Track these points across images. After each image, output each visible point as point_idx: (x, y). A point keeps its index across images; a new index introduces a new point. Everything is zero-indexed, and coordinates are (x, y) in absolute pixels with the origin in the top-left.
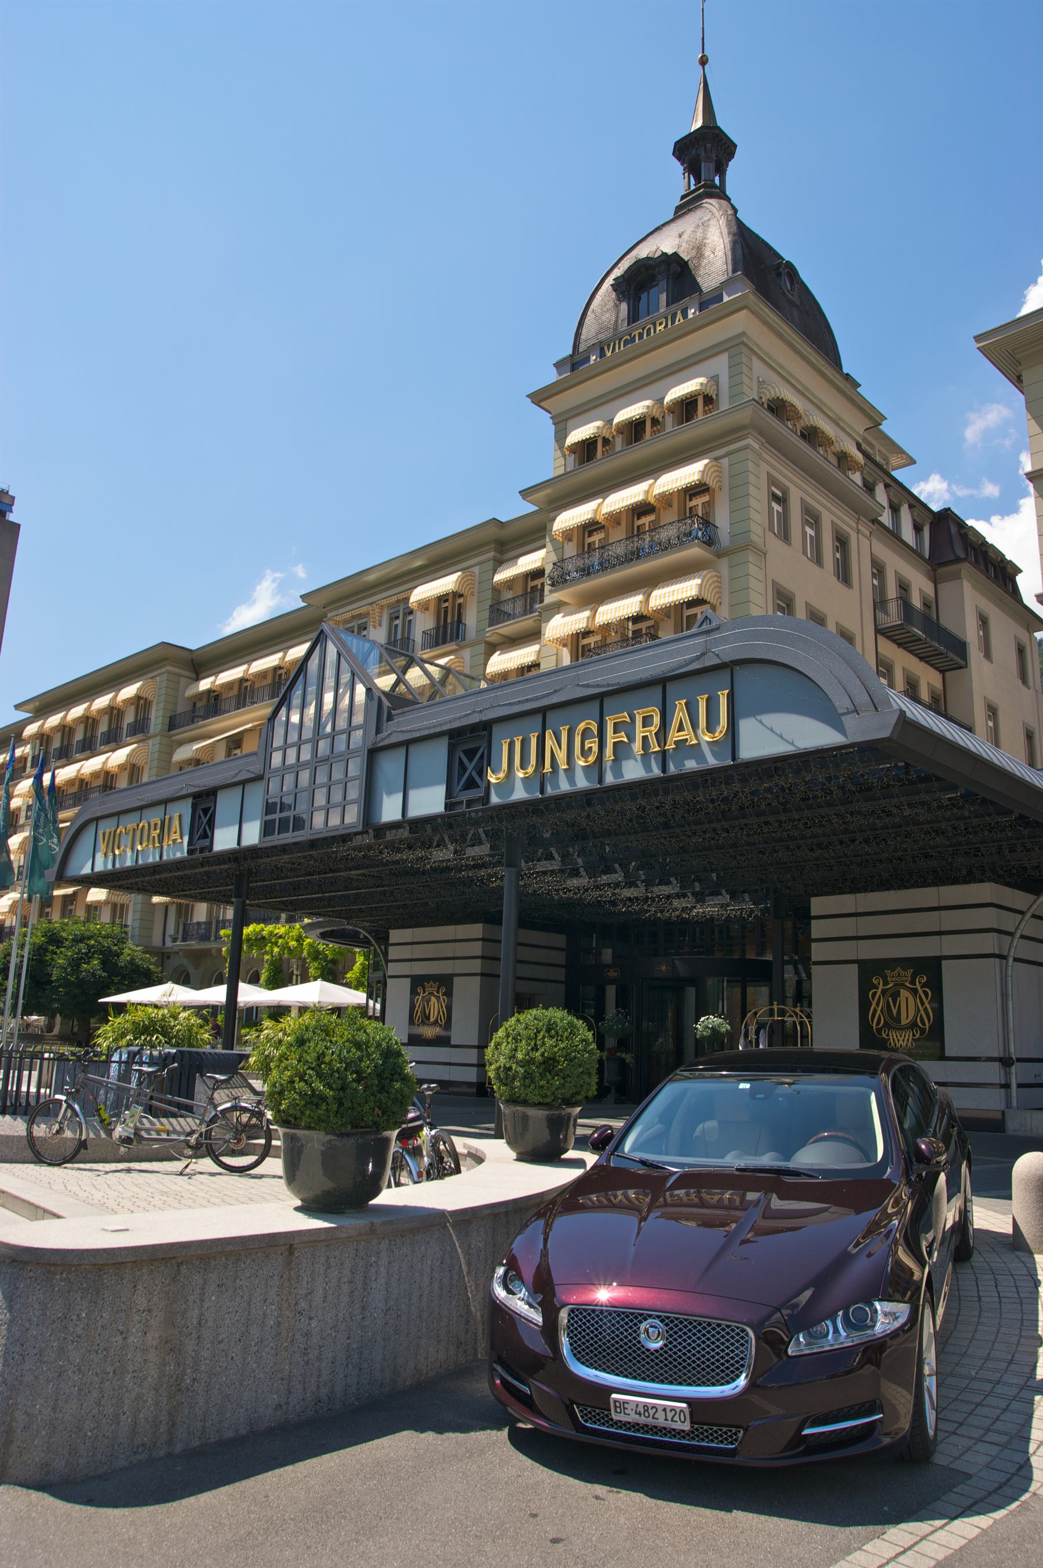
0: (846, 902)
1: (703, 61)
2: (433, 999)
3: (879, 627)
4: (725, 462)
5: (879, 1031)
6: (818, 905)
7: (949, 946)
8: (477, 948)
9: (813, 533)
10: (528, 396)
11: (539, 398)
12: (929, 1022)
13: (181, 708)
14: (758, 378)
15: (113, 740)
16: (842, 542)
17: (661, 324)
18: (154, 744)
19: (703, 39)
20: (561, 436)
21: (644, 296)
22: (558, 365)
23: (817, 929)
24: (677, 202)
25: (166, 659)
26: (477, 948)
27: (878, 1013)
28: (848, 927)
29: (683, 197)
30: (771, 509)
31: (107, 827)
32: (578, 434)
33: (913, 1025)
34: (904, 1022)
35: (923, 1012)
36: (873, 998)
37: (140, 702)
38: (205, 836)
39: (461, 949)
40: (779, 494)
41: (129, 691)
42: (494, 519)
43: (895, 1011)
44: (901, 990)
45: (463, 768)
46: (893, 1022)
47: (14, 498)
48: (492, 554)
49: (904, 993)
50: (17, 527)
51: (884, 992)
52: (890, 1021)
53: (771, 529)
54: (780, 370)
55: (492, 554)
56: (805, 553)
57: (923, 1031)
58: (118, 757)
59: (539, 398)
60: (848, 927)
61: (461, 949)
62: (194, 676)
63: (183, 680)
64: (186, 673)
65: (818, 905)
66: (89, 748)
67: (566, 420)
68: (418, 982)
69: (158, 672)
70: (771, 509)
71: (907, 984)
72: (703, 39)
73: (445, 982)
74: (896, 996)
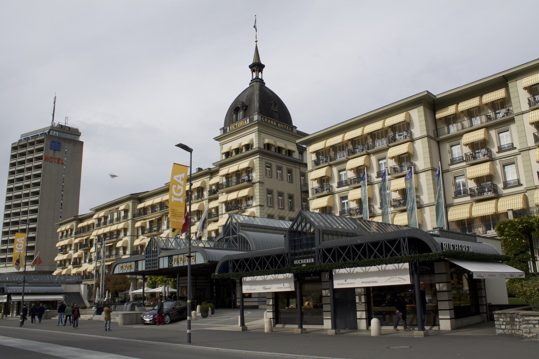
1: (256, 41)
9: (280, 172)
13: (137, 212)
16: (290, 171)
18: (130, 222)
21: (239, 114)
22: (221, 129)
29: (251, 81)
30: (266, 170)
31: (121, 265)
38: (137, 268)
40: (269, 165)
47: (81, 133)
50: (82, 143)
53: (266, 175)
55: (209, 176)
62: (139, 202)
63: (136, 203)
64: (137, 201)
70: (266, 170)
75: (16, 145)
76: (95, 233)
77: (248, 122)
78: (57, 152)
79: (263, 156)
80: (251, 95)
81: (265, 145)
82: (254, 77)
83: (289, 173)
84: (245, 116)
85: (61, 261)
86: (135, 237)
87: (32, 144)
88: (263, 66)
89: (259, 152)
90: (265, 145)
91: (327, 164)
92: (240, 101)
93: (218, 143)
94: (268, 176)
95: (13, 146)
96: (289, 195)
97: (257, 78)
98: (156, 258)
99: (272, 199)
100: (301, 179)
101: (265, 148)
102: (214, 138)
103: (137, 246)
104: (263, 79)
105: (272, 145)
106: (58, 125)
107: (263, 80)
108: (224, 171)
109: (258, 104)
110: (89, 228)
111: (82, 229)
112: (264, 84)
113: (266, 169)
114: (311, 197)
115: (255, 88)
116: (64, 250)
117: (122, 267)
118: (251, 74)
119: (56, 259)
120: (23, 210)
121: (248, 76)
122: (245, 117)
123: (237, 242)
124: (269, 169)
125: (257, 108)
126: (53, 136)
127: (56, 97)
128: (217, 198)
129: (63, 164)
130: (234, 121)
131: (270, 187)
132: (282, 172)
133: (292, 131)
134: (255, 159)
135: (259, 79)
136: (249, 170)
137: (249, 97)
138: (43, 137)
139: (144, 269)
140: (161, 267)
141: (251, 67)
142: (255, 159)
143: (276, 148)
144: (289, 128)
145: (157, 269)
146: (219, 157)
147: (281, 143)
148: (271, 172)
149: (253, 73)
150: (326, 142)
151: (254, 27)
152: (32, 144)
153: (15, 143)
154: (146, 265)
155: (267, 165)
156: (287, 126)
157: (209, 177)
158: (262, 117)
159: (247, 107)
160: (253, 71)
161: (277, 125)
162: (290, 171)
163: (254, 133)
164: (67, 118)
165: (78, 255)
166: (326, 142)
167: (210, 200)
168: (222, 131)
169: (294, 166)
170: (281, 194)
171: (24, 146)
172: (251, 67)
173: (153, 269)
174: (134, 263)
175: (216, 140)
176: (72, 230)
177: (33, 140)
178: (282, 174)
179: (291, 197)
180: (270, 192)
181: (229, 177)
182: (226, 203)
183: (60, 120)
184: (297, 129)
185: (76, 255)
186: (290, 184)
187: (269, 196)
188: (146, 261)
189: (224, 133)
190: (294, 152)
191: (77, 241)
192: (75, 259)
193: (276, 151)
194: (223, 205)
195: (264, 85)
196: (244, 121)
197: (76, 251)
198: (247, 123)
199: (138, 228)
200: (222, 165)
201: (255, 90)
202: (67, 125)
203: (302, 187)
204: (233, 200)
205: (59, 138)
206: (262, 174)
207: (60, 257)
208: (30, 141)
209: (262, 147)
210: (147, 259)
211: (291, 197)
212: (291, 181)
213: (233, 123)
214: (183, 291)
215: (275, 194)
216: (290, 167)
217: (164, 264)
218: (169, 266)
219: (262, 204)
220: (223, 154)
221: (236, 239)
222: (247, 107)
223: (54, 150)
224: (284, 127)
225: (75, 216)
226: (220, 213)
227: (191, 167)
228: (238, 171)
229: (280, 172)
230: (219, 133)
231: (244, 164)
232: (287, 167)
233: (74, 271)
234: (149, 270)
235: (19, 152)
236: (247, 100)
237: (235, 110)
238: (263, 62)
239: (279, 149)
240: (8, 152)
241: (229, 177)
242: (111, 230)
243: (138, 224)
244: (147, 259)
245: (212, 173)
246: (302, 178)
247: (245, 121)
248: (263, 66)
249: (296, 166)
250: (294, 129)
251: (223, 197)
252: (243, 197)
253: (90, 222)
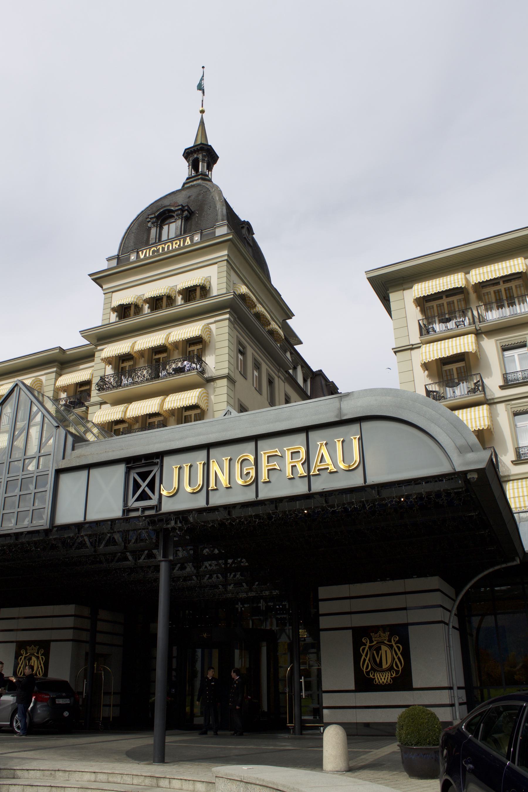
0: (344, 590)
1: (202, 112)
2: (34, 658)
5: (368, 673)
6: (323, 592)
7: (412, 616)
10: (89, 275)
12: (401, 666)
16: (271, 382)
17: (176, 243)
19: (202, 101)
23: (323, 607)
27: (367, 661)
28: (345, 606)
29: (188, 179)
33: (391, 669)
34: (385, 666)
35: (397, 660)
36: (363, 652)
43: (378, 660)
44: (382, 646)
45: (137, 486)
46: (377, 666)
49: (384, 648)
51: (370, 647)
52: (375, 667)
55: (55, 369)
56: (253, 385)
57: (397, 672)
60: (345, 606)
65: (323, 592)
71: (386, 642)
72: (202, 101)
74: (378, 649)
102: (90, 275)
122: (185, 232)
134: (216, 322)
141: (188, 154)
142: (216, 322)
151: (200, 87)
159: (191, 213)
163: (216, 266)
189: (118, 264)
218: (127, 510)
220: (114, 310)
222: (191, 213)
237: (158, 217)
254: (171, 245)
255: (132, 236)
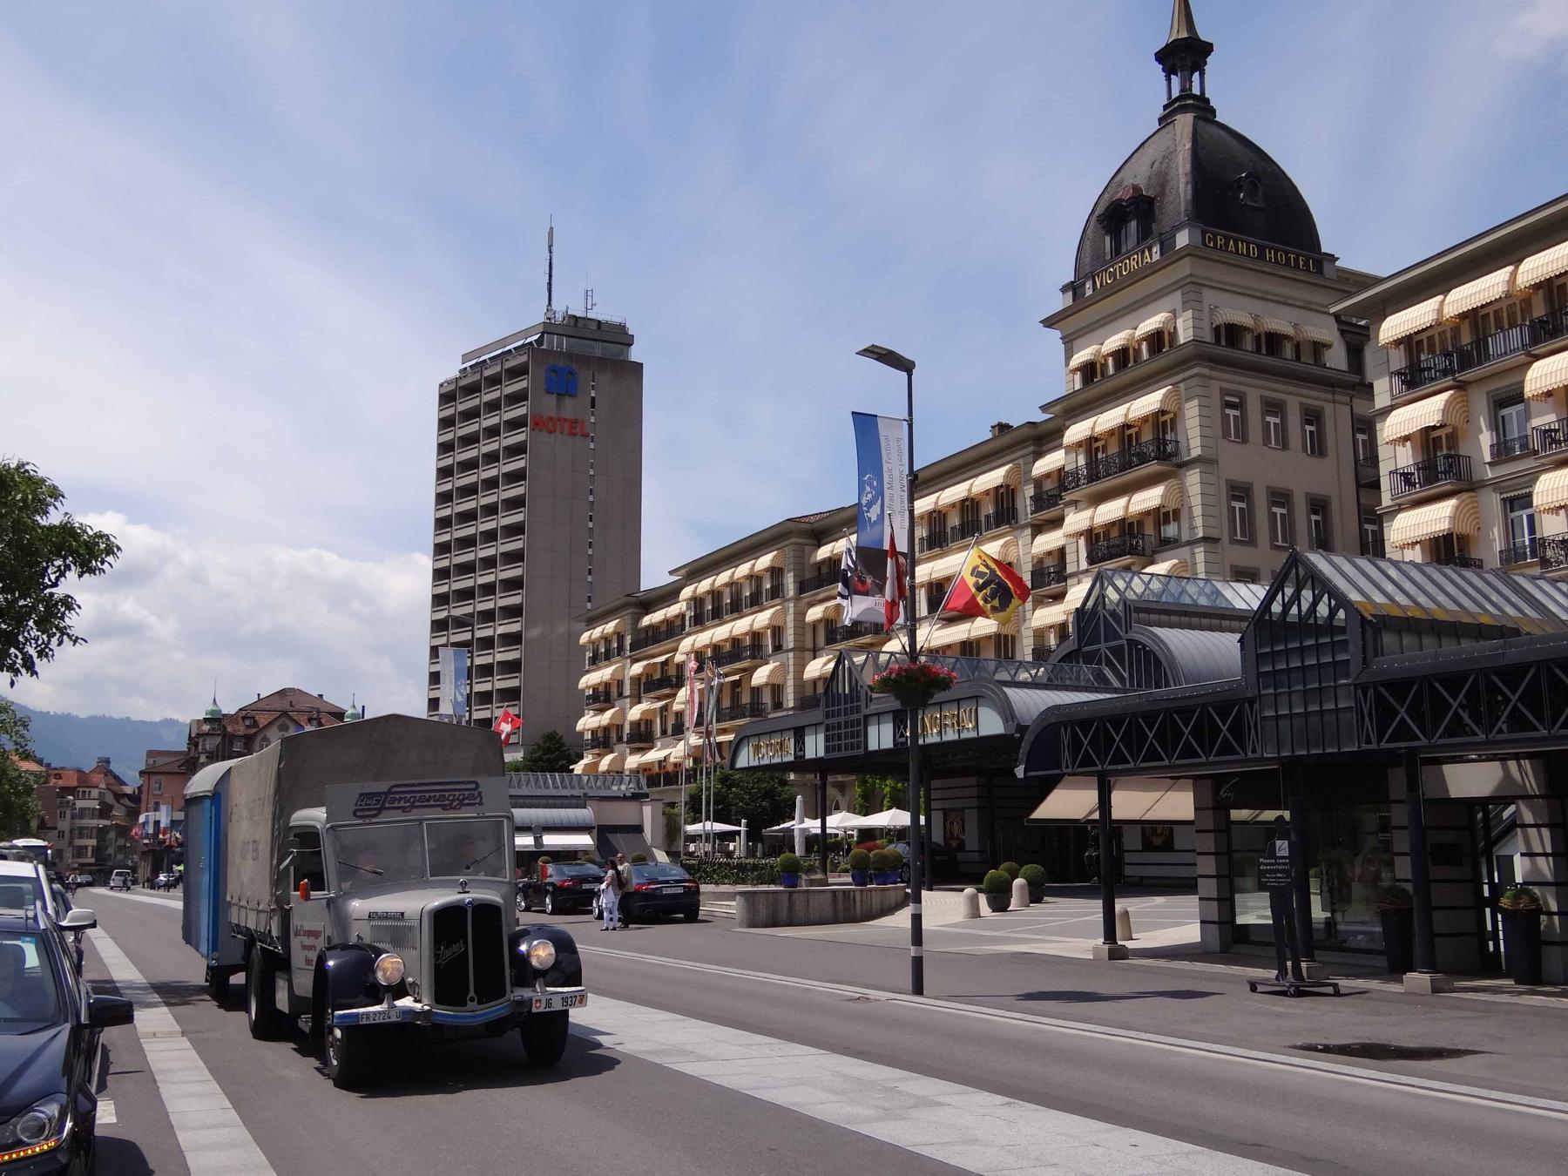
3: (1362, 482)
4: (1182, 386)
8: (974, 792)
11: (1049, 322)
14: (1210, 306)
15: (756, 602)
16: (1312, 416)
20: (1069, 357)
21: (1123, 231)
22: (1064, 290)
24: (1160, 112)
25: (791, 532)
26: (974, 792)
29: (1165, 107)
30: (1225, 418)
31: (754, 741)
32: (1082, 356)
37: (775, 572)
38: (801, 750)
39: (967, 792)
40: (1237, 400)
41: (765, 561)
42: (1028, 423)
48: (1031, 449)
53: (1226, 434)
54: (1233, 289)
55: (1031, 449)
58: (762, 619)
59: (1049, 322)
61: (967, 792)
62: (815, 542)
63: (807, 549)
66: (736, 609)
67: (1072, 340)
68: (946, 812)
69: (786, 543)
70: (1225, 418)
73: (960, 811)
75: (453, 387)
76: (686, 644)
77: (1156, 257)
78: (569, 403)
79: (1211, 368)
80: (1164, 157)
81: (1217, 330)
82: (1176, 93)
83: (1309, 423)
84: (1145, 235)
85: (594, 732)
86: (808, 655)
87: (495, 381)
88: (1207, 49)
89: (1198, 355)
90: (1217, 330)
91: (1448, 381)
92: (1125, 183)
93: (1055, 335)
94: (1233, 438)
95: (444, 390)
96: (1311, 499)
97: (1186, 93)
98: (854, 717)
99: (1248, 516)
100: (1355, 441)
101: (1218, 342)
103: (815, 682)
104: (1206, 96)
105: (1246, 329)
106: (564, 319)
107: (1208, 101)
108: (1077, 431)
109: (1190, 187)
110: (672, 630)
111: (650, 634)
112: (1213, 111)
113: (1223, 412)
114: (1390, 503)
115: (1178, 133)
116: (603, 697)
117: (757, 749)
118: (1165, 83)
119: (580, 726)
120: (481, 581)
121: (1155, 89)
123: (1123, 666)
124: (1237, 413)
125: (1186, 205)
126: (549, 352)
127: (552, 229)
128: (1057, 522)
129: (585, 435)
130: (1108, 257)
131: (1239, 476)
132: (1284, 420)
133: (1320, 271)
135: (1194, 97)
136: (1162, 422)
137: (1156, 165)
138: (524, 358)
139: (821, 753)
140: (873, 746)
141: (1161, 57)
143: (1258, 338)
144: (1306, 264)
145: (861, 751)
146: (1062, 382)
147: (1278, 321)
148: (1242, 423)
149: (1169, 80)
150: (1442, 302)
152: (495, 381)
153: (449, 382)
154: (827, 739)
155: (1227, 398)
156: (1298, 256)
157: (1033, 452)
158: (1204, 233)
159: (1150, 201)
160: (1169, 72)
161: (1261, 256)
162: (1312, 416)
164: (590, 293)
165: (643, 713)
166: (1442, 302)
167: (1038, 529)
168: (1070, 294)
169: (1329, 397)
170: (1280, 497)
171: (472, 389)
172: (1161, 57)
173: (849, 753)
174: (791, 733)
175: (1049, 327)
176: (621, 638)
177: (498, 369)
178: (1282, 430)
179: (1319, 505)
180: (1239, 491)
181: (1097, 449)
182: (1091, 535)
183: (570, 303)
184: (1337, 263)
185: (635, 713)
186: (1314, 462)
187: (1237, 505)
188: (827, 729)
190: (1328, 346)
191: (637, 668)
192: (636, 725)
193: (1258, 350)
194: (1082, 541)
195: (1210, 116)
196: (1143, 252)
197: (637, 700)
198: (1151, 259)
199: (815, 625)
200: (1073, 408)
201: (1178, 138)
202: (590, 316)
203: (1360, 468)
204: (1113, 524)
205: (570, 356)
206: (1209, 432)
207: (589, 722)
208: (487, 373)
209: (1208, 337)
210: (830, 721)
211: (1319, 505)
212: (1318, 447)
213: (1105, 262)
214: (952, 823)
215: (1260, 500)
216: (1310, 401)
217: (881, 737)
219: (1214, 533)
220: (1074, 371)
221: (1117, 651)
223: (559, 395)
224: (1288, 260)
225: (628, 595)
226: (1070, 568)
227: (911, 420)
228: (1126, 426)
229: (1277, 421)
230: (1060, 302)
231: (1147, 403)
232: (1300, 403)
233: (633, 761)
234: (836, 755)
235: (461, 408)
236: (1150, 178)
238: (1204, 35)
239: (1273, 342)
240: (430, 412)
241: (1097, 449)
242: (735, 633)
243: (815, 613)
244: (830, 721)
245: (1042, 438)
246: (1360, 437)
247: (1147, 253)
248: (1207, 49)
249: (1338, 397)
250: (1326, 265)
251: (1076, 520)
252: (1148, 513)
253: (673, 610)
254: (1128, 261)
255: (1087, 245)
